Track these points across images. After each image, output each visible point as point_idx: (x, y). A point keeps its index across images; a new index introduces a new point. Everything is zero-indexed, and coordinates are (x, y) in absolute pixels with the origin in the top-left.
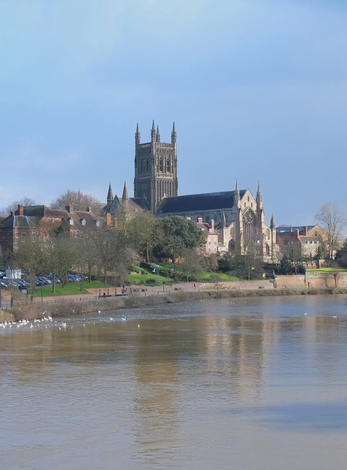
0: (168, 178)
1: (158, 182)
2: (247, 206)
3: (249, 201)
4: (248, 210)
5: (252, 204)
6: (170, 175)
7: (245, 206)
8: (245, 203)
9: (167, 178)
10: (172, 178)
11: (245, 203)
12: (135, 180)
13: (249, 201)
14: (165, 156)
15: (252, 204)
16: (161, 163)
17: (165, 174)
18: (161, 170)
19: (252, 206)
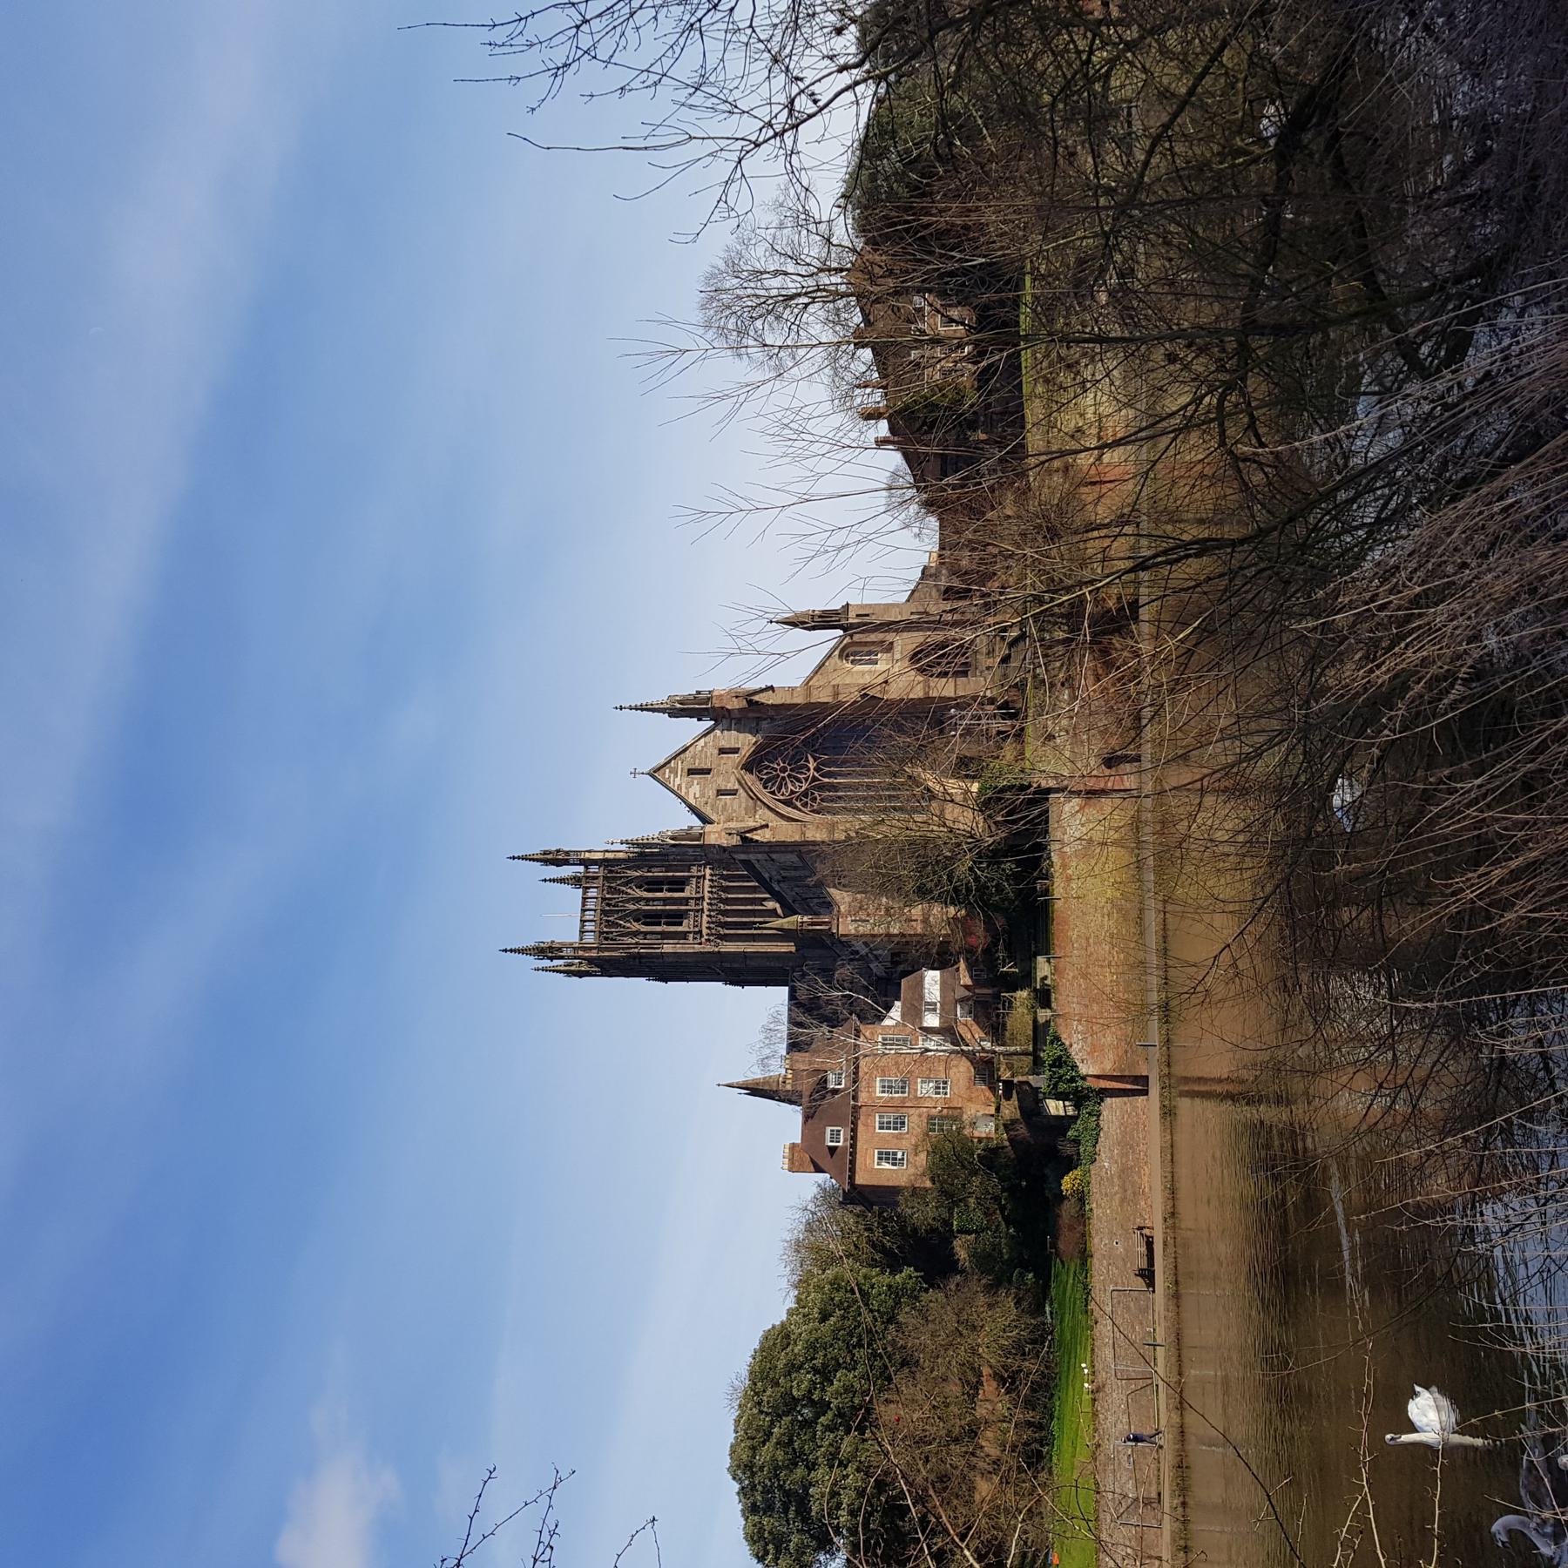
0: (707, 889)
3: (708, 771)
6: (699, 877)
9: (707, 895)
10: (708, 871)
13: (708, 771)
14: (628, 901)
16: (652, 918)
18: (676, 918)
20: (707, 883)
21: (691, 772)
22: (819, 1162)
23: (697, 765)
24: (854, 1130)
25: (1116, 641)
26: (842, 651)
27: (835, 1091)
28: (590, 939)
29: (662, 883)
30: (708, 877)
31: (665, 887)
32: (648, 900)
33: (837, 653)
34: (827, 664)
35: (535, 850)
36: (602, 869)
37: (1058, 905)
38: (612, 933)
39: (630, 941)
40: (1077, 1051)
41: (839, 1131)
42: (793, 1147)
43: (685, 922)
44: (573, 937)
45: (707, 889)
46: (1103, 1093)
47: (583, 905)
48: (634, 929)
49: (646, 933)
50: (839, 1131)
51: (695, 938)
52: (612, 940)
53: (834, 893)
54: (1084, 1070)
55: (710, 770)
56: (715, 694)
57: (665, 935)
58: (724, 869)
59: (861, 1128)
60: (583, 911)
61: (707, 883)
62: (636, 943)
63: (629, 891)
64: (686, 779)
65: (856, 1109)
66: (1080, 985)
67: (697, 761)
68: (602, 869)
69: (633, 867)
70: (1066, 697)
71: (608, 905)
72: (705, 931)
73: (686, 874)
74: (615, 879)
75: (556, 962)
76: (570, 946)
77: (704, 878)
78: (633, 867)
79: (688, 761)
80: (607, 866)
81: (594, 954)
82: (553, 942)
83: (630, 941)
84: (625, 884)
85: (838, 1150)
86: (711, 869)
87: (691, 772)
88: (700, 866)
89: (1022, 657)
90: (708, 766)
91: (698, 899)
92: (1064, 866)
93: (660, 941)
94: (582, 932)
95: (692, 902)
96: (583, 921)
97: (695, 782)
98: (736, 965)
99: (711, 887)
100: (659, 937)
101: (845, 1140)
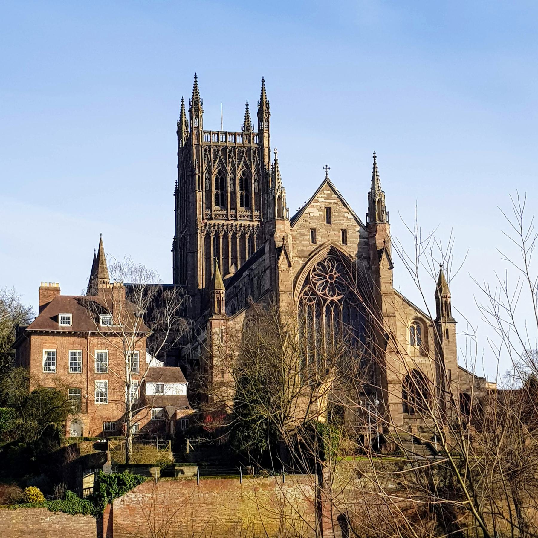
0: (243, 223)
1: (208, 237)
2: (320, 240)
3: (329, 221)
4: (324, 253)
5: (344, 232)
6: (251, 217)
7: (314, 241)
8: (314, 231)
9: (239, 223)
10: (256, 223)
11: (314, 231)
12: (175, 244)
13: (329, 221)
14: (233, 165)
15: (344, 232)
16: (221, 184)
17: (231, 212)
18: (222, 202)
19: (345, 241)
20: (248, 223)
21: (328, 209)
22: (46, 310)
23: (334, 214)
24: (70, 334)
25: (433, 523)
26: (421, 320)
27: (97, 320)
28: (205, 139)
29: (247, 190)
30: (252, 223)
31: (244, 192)
32: (234, 180)
33: (419, 315)
34: (411, 308)
35: (269, 97)
36: (257, 146)
37: (236, 482)
38: (210, 155)
39: (204, 168)
40: (129, 497)
41: (69, 324)
42: (57, 290)
43: (219, 208)
44: (206, 127)
45: (243, 223)
46: (99, 516)
47: (230, 133)
48: (213, 170)
49: (210, 179)
50: (69, 324)
51: (207, 215)
52: (205, 154)
53: (241, 317)
54: (116, 502)
55: (331, 224)
56: (387, 226)
57: (209, 193)
58: (258, 235)
59: (72, 339)
60: (226, 133)
61: (248, 223)
62: (202, 173)
63: (241, 166)
64: (323, 205)
65: (85, 335)
66: (178, 499)
67: (336, 214)
68: (257, 146)
69: (258, 169)
70: (390, 486)
71: (230, 151)
72: (212, 222)
73: (254, 207)
74: (249, 156)
75: (188, 115)
76: (200, 124)
77: (250, 221)
78: (258, 169)
79: (337, 208)
80: (258, 150)
81: (194, 142)
82: (202, 111)
83: (204, 168)
84: (245, 163)
85: (55, 323)
86: (258, 227)
87: (328, 209)
88: (260, 218)
89: (419, 453)
90: (333, 222)
91: (236, 216)
92: (265, 486)
93: (204, 190)
94: (210, 132)
95: (233, 212)
96: (218, 133)
97: (321, 213)
98: (188, 245)
99: (244, 226)
100: (208, 189)
101: (63, 328)
